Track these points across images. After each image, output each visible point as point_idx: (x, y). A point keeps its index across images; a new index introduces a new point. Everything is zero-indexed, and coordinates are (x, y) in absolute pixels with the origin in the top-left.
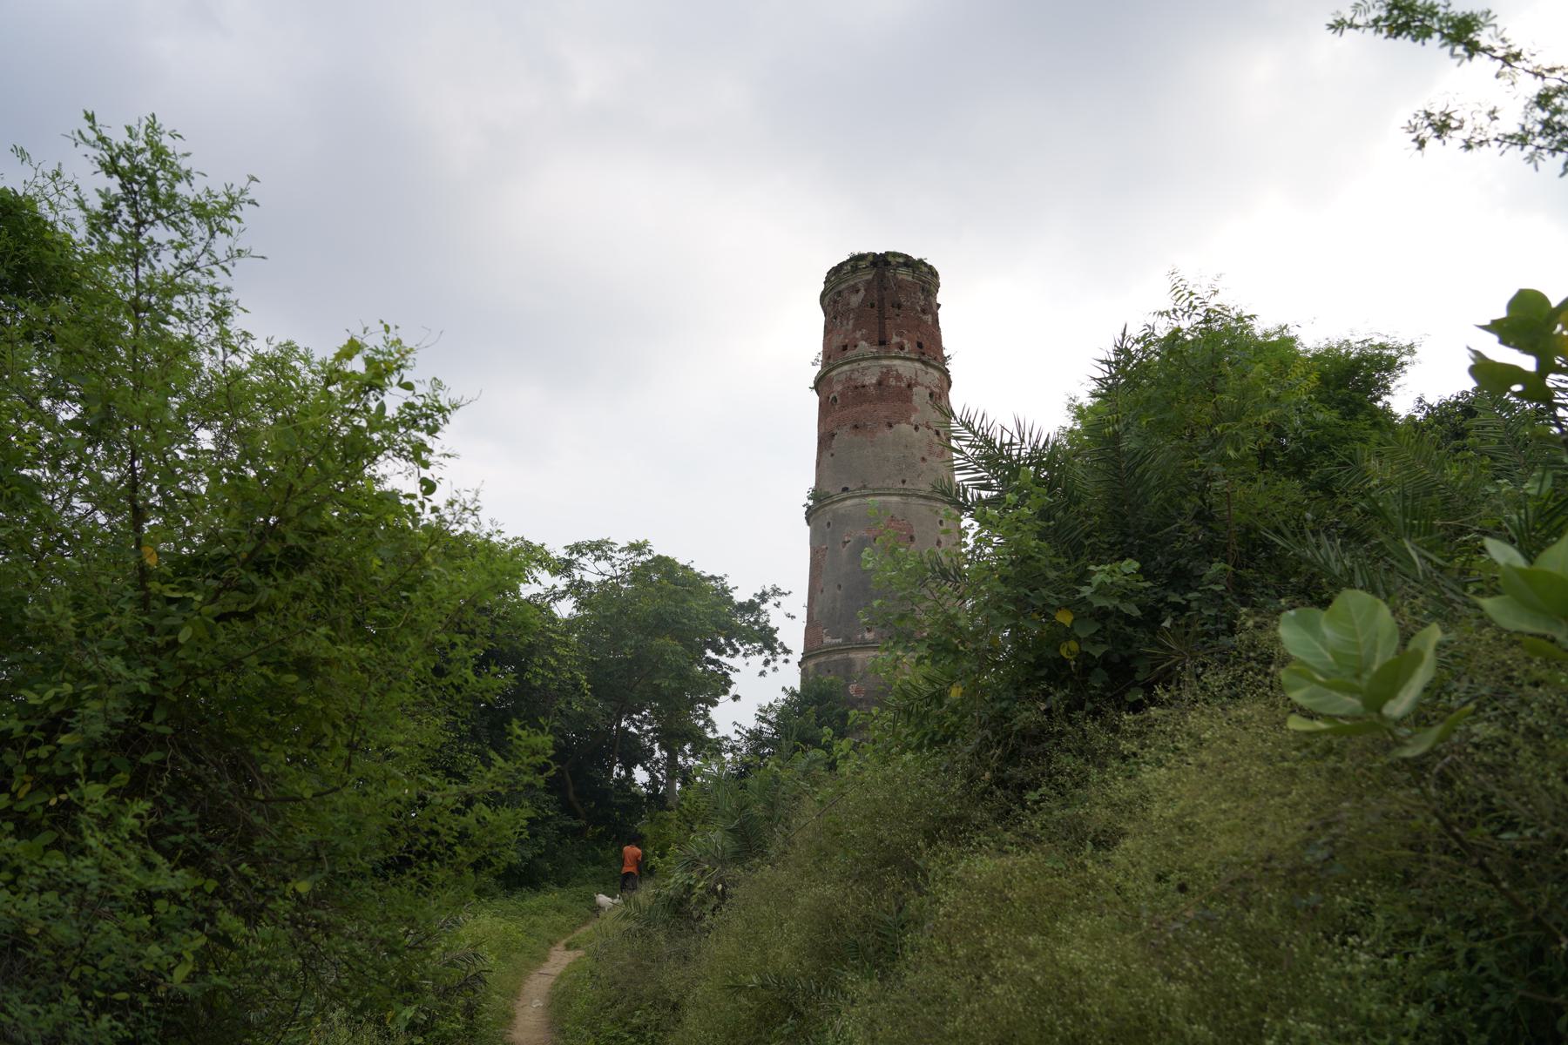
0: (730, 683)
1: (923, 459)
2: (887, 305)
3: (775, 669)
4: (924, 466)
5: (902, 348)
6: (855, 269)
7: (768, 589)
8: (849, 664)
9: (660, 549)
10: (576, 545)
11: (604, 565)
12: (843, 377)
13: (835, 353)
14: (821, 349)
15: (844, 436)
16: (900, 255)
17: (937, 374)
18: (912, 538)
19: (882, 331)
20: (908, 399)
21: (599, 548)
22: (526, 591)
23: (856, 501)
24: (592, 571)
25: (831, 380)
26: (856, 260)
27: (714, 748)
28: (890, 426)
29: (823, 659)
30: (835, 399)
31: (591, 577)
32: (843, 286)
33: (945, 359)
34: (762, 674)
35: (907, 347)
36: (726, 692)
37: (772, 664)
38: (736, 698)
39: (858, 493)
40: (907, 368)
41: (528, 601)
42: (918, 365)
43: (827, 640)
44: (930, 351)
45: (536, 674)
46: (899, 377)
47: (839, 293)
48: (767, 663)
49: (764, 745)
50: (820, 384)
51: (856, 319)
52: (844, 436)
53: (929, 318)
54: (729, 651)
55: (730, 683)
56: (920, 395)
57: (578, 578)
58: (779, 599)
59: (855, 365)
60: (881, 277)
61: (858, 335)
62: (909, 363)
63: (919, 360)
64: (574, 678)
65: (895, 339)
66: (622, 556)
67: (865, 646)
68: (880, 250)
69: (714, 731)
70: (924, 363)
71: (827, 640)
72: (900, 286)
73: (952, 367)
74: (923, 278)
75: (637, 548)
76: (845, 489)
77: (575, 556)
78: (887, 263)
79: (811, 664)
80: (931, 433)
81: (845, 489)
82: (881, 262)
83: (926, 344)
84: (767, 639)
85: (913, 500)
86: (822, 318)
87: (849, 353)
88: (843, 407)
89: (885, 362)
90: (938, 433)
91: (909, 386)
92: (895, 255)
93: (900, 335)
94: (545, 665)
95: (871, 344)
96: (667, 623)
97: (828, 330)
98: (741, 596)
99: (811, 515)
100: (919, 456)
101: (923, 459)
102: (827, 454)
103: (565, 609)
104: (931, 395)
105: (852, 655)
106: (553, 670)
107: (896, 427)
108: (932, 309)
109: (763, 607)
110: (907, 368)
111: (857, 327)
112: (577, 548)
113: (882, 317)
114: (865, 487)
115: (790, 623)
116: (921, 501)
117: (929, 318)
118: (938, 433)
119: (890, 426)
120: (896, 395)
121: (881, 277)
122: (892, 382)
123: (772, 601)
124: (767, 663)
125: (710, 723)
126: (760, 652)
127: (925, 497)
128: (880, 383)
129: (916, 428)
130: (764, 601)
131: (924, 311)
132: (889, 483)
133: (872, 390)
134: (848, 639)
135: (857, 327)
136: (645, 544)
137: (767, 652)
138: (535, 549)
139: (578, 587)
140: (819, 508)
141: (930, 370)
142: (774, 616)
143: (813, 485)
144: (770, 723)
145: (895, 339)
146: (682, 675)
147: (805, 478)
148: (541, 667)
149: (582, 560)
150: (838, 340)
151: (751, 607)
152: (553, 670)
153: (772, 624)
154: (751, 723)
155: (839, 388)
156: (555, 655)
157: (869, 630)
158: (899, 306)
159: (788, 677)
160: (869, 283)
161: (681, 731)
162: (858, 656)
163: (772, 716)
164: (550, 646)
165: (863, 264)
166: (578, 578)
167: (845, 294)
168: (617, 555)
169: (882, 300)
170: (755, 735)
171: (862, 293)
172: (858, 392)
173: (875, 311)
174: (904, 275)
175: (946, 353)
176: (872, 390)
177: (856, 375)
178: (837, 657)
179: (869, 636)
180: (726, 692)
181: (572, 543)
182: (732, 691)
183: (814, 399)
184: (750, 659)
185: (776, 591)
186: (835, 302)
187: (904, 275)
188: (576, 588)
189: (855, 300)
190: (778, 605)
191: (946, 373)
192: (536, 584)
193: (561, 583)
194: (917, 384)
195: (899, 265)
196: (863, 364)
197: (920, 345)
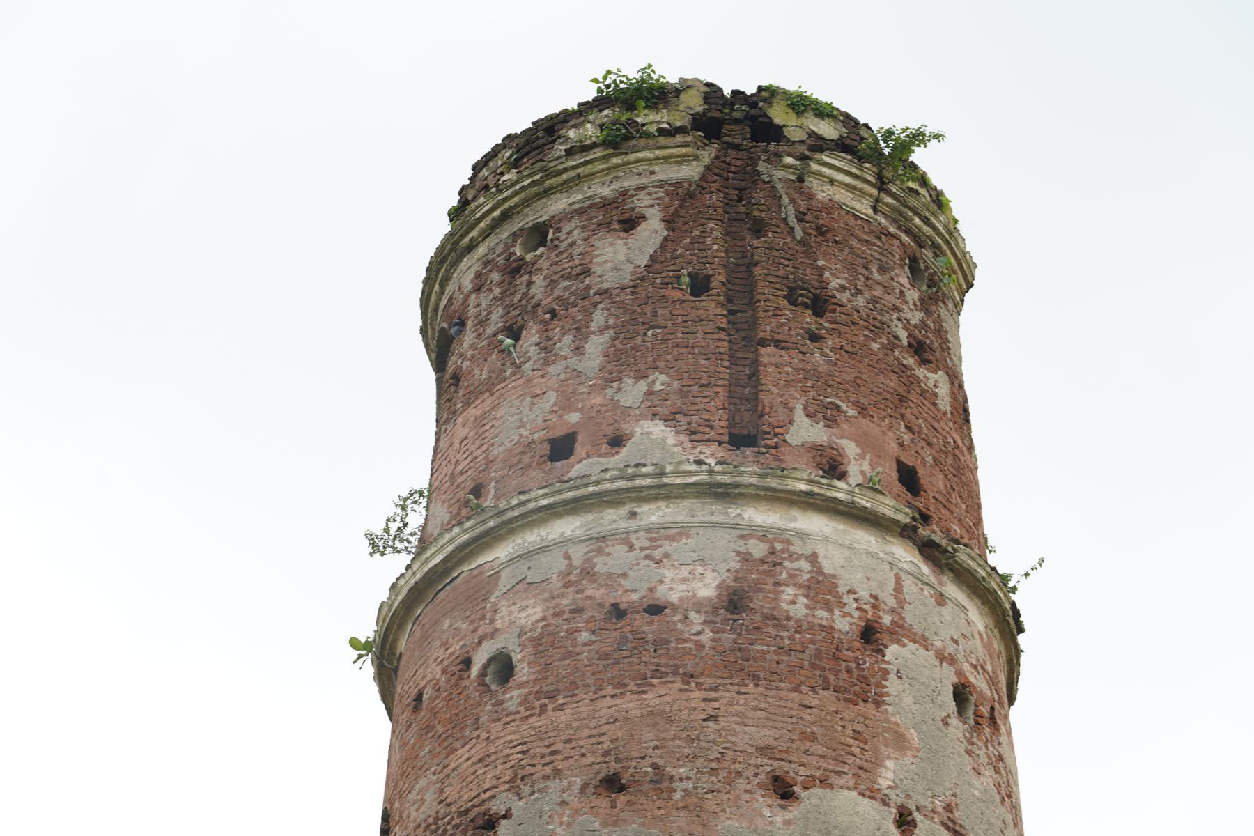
2: (769, 293)
5: (834, 469)
12: (552, 565)
16: (824, 111)
17: (978, 619)
20: (866, 690)
25: (484, 586)
26: (630, 105)
28: (784, 791)
30: (503, 668)
32: (559, 204)
35: (857, 469)
42: (905, 554)
44: (934, 507)
46: (821, 588)
47: (539, 235)
53: (936, 380)
56: (913, 683)
59: (612, 518)
61: (632, 393)
62: (865, 538)
63: (906, 533)
65: (805, 431)
68: (738, 78)
70: (929, 550)
72: (822, 226)
78: (768, 132)
82: (742, 126)
83: (933, 482)
87: (586, 466)
88: (546, 695)
91: (869, 634)
92: (801, 104)
104: (961, 694)
107: (811, 798)
108: (934, 348)
110: (867, 563)
111: (621, 362)
113: (745, 338)
128: (733, 602)
129: (904, 821)
135: (621, 362)
141: (952, 590)
150: (520, 417)
155: (530, 613)
158: (820, 304)
167: (572, 232)
169: (742, 275)
171: (652, 231)
173: (712, 307)
174: (837, 185)
177: (615, 559)
186: (515, 269)
189: (618, 258)
191: (1008, 623)
194: (900, 632)
195: (819, 144)
196: (655, 514)
197: (909, 479)
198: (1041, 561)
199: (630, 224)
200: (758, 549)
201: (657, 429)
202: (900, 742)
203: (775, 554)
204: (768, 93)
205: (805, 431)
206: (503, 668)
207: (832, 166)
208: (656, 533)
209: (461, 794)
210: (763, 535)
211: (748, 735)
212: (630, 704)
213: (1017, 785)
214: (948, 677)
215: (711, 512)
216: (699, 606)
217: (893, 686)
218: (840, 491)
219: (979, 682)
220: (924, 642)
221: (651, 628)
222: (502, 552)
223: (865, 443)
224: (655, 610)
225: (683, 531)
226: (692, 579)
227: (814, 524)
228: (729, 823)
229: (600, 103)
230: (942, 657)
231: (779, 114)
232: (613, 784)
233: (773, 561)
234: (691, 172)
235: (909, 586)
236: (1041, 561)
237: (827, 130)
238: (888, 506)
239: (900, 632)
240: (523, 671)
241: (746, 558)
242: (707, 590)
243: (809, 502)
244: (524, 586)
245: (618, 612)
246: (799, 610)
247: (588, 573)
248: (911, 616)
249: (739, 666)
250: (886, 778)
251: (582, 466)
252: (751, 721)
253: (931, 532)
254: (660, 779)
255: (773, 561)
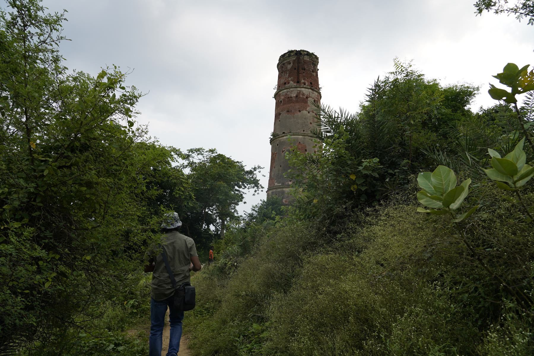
0: (243, 198)
1: (311, 123)
2: (300, 69)
3: (258, 193)
5: (305, 84)
6: (289, 56)
7: (256, 167)
8: (283, 192)
9: (220, 151)
10: (191, 150)
11: (200, 157)
12: (284, 94)
13: (282, 85)
14: (276, 83)
15: (284, 114)
16: (306, 51)
17: (316, 94)
18: (306, 150)
19: (298, 78)
20: (306, 102)
21: (199, 151)
22: (174, 164)
24: (196, 159)
25: (280, 95)
26: (290, 52)
27: (237, 219)
28: (300, 111)
29: (274, 190)
30: (281, 101)
31: (196, 161)
32: (285, 62)
33: (319, 89)
34: (254, 195)
35: (307, 84)
36: (242, 201)
37: (257, 192)
38: (245, 203)
40: (306, 91)
41: (174, 168)
42: (310, 90)
43: (276, 184)
44: (314, 85)
45: (177, 193)
46: (303, 94)
48: (255, 191)
49: (253, 219)
50: (276, 96)
51: (289, 74)
52: (284, 114)
53: (315, 74)
54: (243, 187)
55: (243, 198)
57: (191, 161)
58: (260, 170)
59: (288, 90)
60: (298, 59)
61: (290, 79)
62: (307, 90)
63: (310, 89)
64: (190, 194)
66: (207, 153)
67: (288, 186)
69: (237, 214)
70: (312, 89)
71: (276, 184)
72: (305, 62)
73: (322, 91)
74: (313, 60)
75: (212, 151)
76: (284, 133)
77: (190, 153)
78: (301, 54)
79: (270, 192)
81: (284, 133)
82: (299, 54)
83: (313, 83)
84: (256, 183)
86: (278, 73)
88: (284, 104)
89: (299, 89)
91: (307, 98)
92: (304, 51)
93: (304, 79)
94: (180, 190)
95: (294, 82)
96: (222, 176)
97: (280, 77)
98: (247, 169)
99: (272, 141)
100: (309, 122)
101: (311, 123)
102: (278, 121)
103: (187, 171)
104: (314, 101)
105: (284, 189)
106: (183, 192)
108: (316, 71)
109: (255, 172)
110: (306, 91)
111: (289, 76)
112: (191, 151)
113: (298, 73)
114: (290, 132)
115: (264, 178)
116: (309, 138)
117: (315, 74)
119: (300, 111)
120: (302, 100)
121: (298, 59)
122: (301, 96)
123: (258, 170)
124: (255, 191)
125: (236, 211)
126: (253, 187)
128: (297, 96)
129: (309, 112)
130: (255, 170)
131: (313, 71)
132: (299, 131)
133: (294, 99)
134: (283, 184)
135: (289, 76)
136: (214, 150)
137: (256, 188)
138: (177, 151)
139: (192, 164)
140: (274, 139)
141: (314, 92)
142: (258, 175)
143: (273, 131)
144: (256, 211)
145: (303, 81)
146: (227, 194)
147: (271, 129)
148: (178, 190)
149: (193, 155)
150: (283, 81)
151: (251, 172)
152: (183, 192)
153: (258, 178)
154: (250, 211)
155: (283, 97)
156: (183, 187)
157: (290, 181)
158: (304, 69)
159: (262, 196)
160: (294, 61)
161: (226, 214)
162: (287, 190)
163: (256, 209)
164: (181, 184)
165: (292, 54)
166: (191, 161)
167: (286, 64)
168: (205, 153)
170: (251, 215)
171: (292, 64)
172: (289, 99)
173: (296, 71)
174: (306, 58)
175: (320, 87)
176: (294, 99)
178: (279, 190)
179: (290, 183)
180: (242, 201)
181: (189, 149)
182: (244, 200)
183: (274, 101)
184: (250, 190)
185: (259, 167)
186: (282, 67)
187: (306, 58)
188: (191, 164)
189: (289, 67)
190: (260, 172)
191: (320, 93)
192: (177, 163)
193: (186, 162)
194: (309, 97)
195: (305, 55)
196: (291, 89)
197: (311, 83)
199: (290, 64)
201: (292, 82)
204: (301, 50)
205: (303, 81)
207: (306, 57)
208: (292, 91)
211: (297, 107)
215: (295, 89)
227: (303, 89)
229: (288, 52)
231: (302, 52)
234: (294, 59)
237: (306, 53)
249: (297, 102)
251: (287, 85)
252: (297, 106)
253: (313, 88)
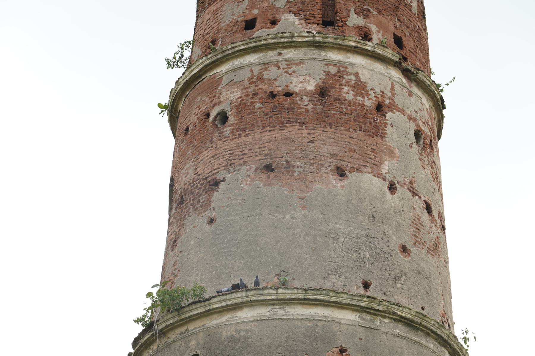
1: (404, 249)
4: (404, 260)
5: (366, 37)
12: (245, 75)
15: (241, 185)
17: (426, 103)
20: (378, 132)
23: (264, 311)
25: (216, 83)
28: (341, 173)
30: (223, 118)
35: (376, 37)
39: (269, 294)
42: (395, 74)
44: (409, 54)
46: (360, 87)
52: (241, 185)
56: (398, 129)
59: (271, 55)
62: (379, 67)
63: (397, 65)
65: (354, 20)
70: (406, 72)
80: (419, 204)
83: (409, 43)
85: (384, 325)
87: (260, 33)
88: (241, 130)
90: (428, 208)
91: (380, 108)
93: (365, 14)
100: (395, 242)
102: (196, 224)
104: (418, 134)
107: (353, 177)
110: (379, 77)
114: (284, 285)
116: (400, 329)
118: (428, 208)
127: (408, 323)
128: (322, 92)
129: (392, 188)
141: (415, 90)
155: (235, 95)
177: (272, 73)
191: (439, 105)
194: (393, 107)
196: (289, 54)
197: (398, 42)
198: (454, 79)
200: (333, 70)
201: (291, 17)
202: (391, 154)
203: (340, 73)
205: (354, 20)
206: (223, 118)
208: (289, 62)
209: (204, 171)
210: (335, 64)
211: (327, 149)
212: (277, 134)
213: (440, 174)
214: (413, 127)
216: (307, 94)
217: (389, 130)
218: (369, 46)
219: (426, 129)
220: (403, 112)
221: (286, 102)
222: (224, 68)
223: (380, 26)
224: (288, 95)
225: (302, 61)
226: (305, 83)
228: (318, 186)
230: (410, 118)
232: (269, 168)
233: (339, 75)
235: (397, 87)
236: (454, 79)
238: (389, 53)
239: (393, 107)
240: (232, 120)
241: (328, 74)
242: (311, 87)
243: (355, 50)
244: (233, 83)
245: (273, 95)
246: (350, 96)
247: (260, 78)
248: (397, 100)
249: (324, 119)
250: (385, 169)
251: (258, 32)
252: (328, 143)
254: (289, 166)
255: (339, 75)
